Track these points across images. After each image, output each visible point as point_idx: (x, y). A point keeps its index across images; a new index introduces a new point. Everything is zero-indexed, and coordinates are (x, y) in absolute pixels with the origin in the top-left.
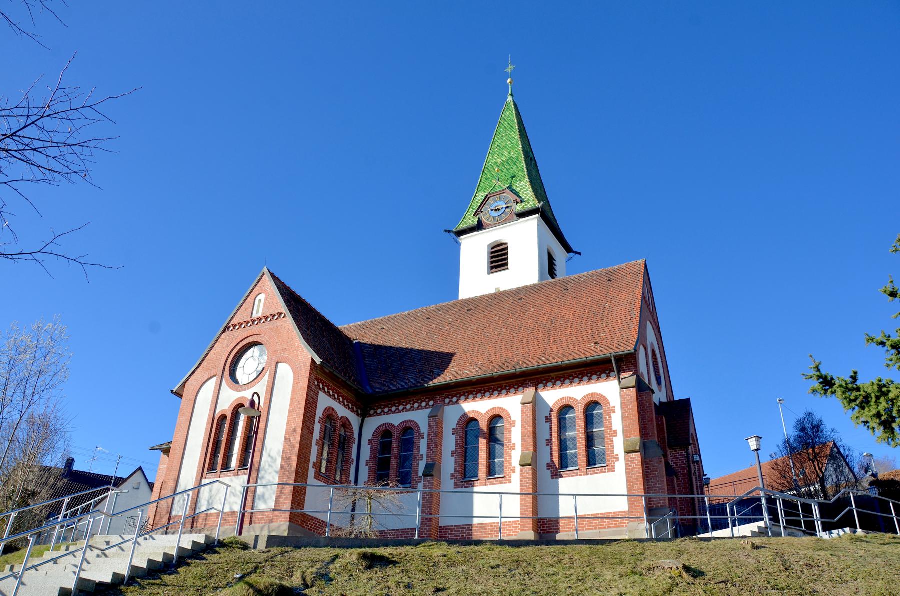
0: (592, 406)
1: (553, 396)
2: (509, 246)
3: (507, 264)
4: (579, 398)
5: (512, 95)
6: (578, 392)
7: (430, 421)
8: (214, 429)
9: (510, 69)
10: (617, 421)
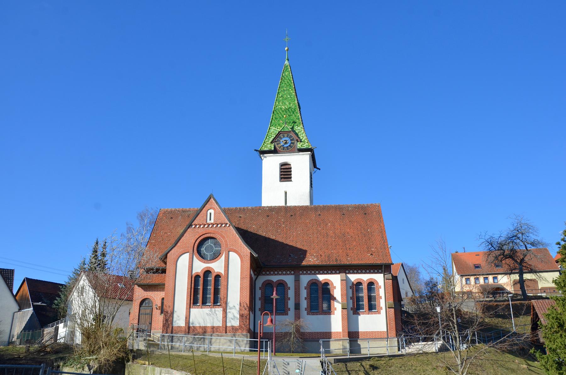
0: (371, 284)
1: (354, 277)
2: (292, 166)
3: (291, 178)
4: (365, 280)
5: (288, 60)
6: (365, 277)
7: (295, 283)
8: (193, 282)
9: (286, 39)
10: (382, 292)
